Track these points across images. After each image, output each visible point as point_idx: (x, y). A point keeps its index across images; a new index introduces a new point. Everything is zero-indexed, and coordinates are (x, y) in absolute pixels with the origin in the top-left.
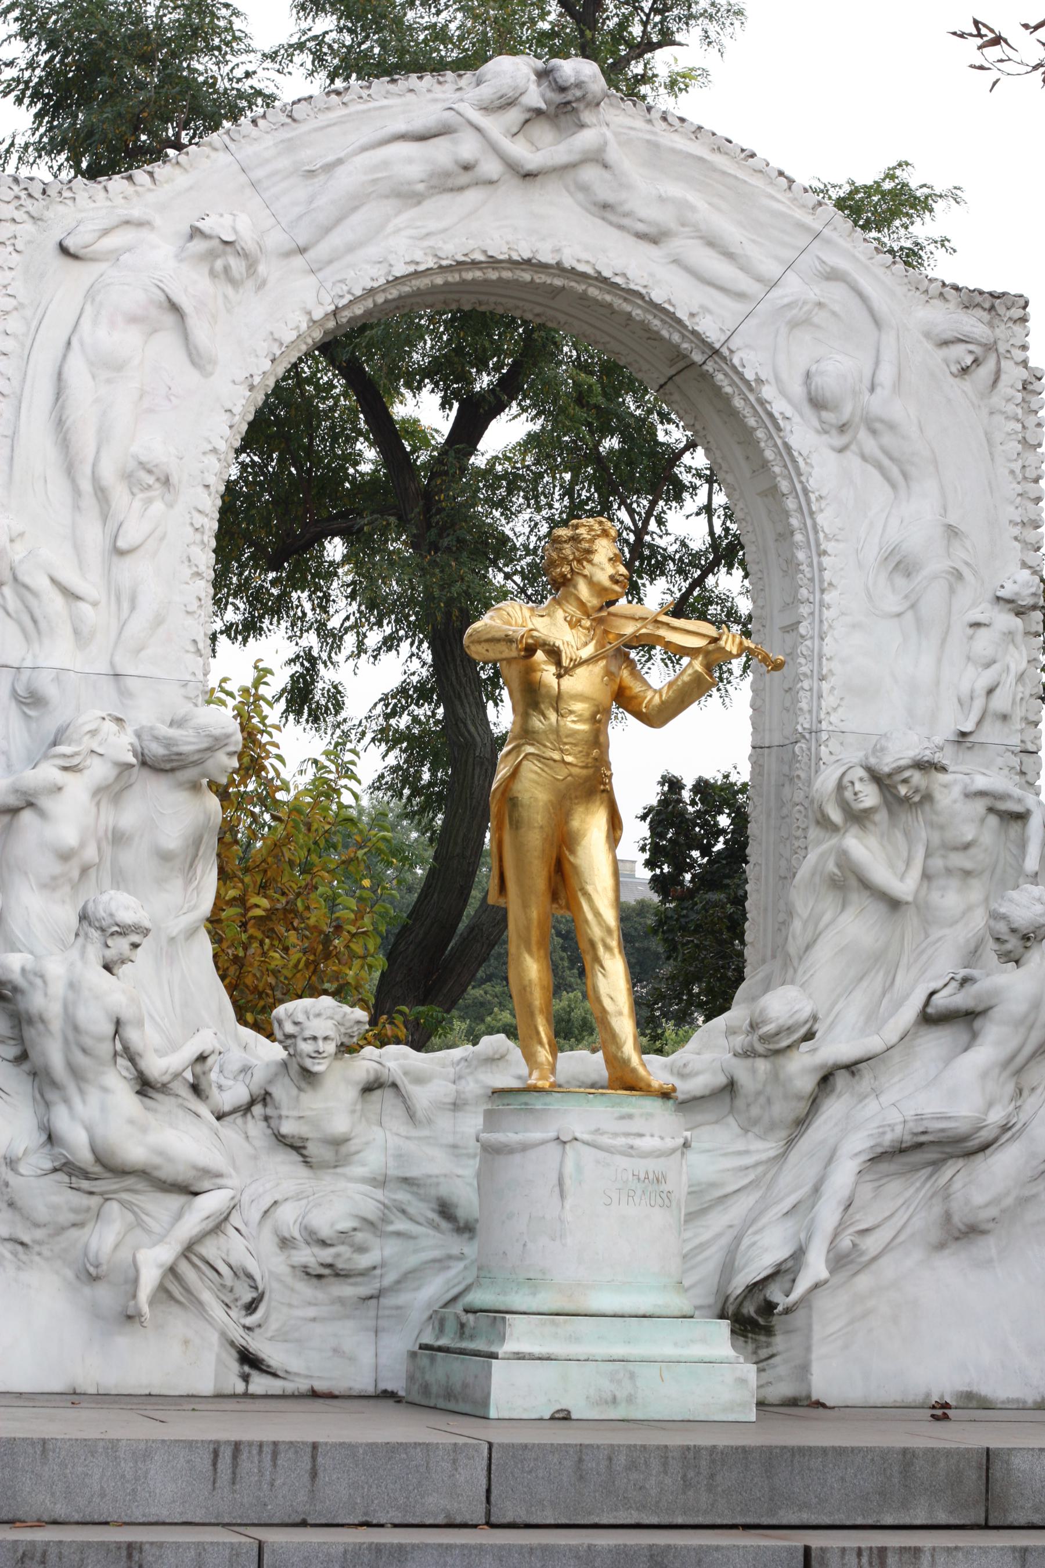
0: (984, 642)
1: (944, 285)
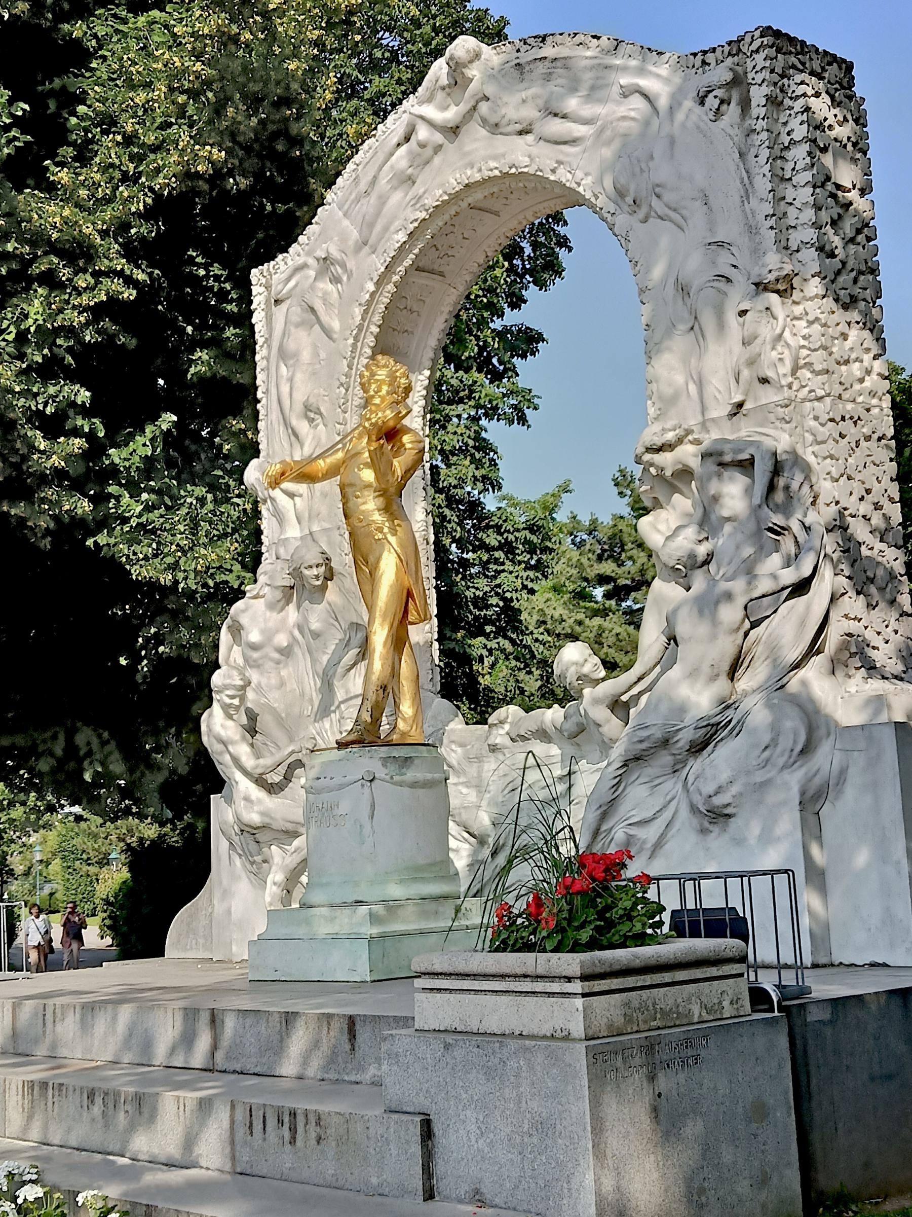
1: (705, 52)
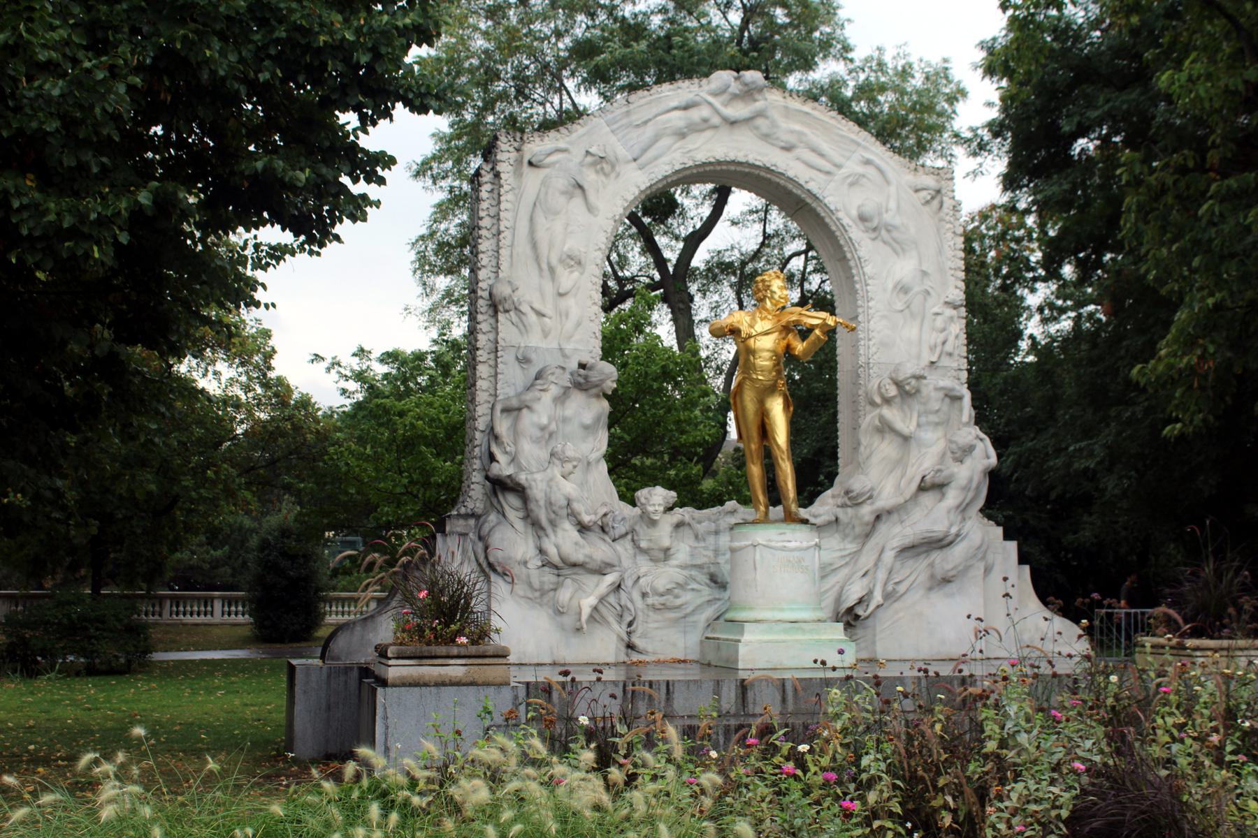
0: (939, 322)
